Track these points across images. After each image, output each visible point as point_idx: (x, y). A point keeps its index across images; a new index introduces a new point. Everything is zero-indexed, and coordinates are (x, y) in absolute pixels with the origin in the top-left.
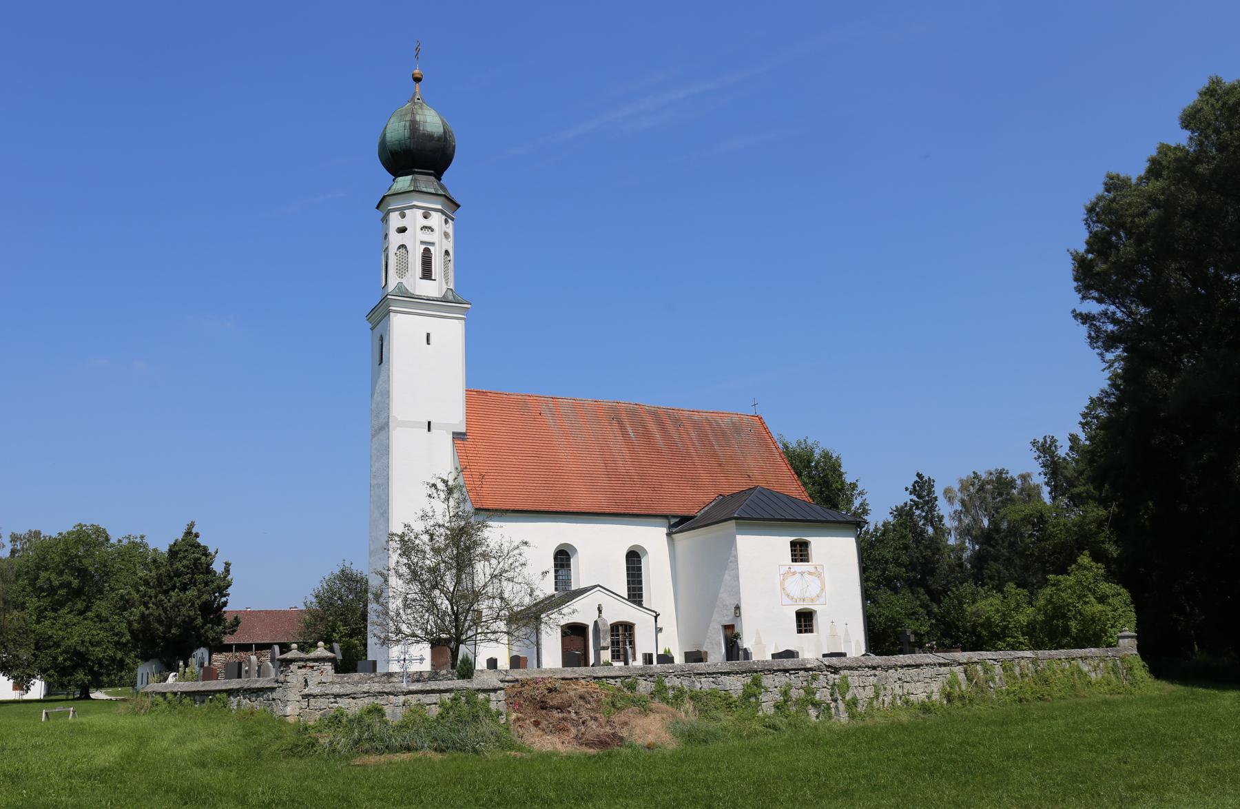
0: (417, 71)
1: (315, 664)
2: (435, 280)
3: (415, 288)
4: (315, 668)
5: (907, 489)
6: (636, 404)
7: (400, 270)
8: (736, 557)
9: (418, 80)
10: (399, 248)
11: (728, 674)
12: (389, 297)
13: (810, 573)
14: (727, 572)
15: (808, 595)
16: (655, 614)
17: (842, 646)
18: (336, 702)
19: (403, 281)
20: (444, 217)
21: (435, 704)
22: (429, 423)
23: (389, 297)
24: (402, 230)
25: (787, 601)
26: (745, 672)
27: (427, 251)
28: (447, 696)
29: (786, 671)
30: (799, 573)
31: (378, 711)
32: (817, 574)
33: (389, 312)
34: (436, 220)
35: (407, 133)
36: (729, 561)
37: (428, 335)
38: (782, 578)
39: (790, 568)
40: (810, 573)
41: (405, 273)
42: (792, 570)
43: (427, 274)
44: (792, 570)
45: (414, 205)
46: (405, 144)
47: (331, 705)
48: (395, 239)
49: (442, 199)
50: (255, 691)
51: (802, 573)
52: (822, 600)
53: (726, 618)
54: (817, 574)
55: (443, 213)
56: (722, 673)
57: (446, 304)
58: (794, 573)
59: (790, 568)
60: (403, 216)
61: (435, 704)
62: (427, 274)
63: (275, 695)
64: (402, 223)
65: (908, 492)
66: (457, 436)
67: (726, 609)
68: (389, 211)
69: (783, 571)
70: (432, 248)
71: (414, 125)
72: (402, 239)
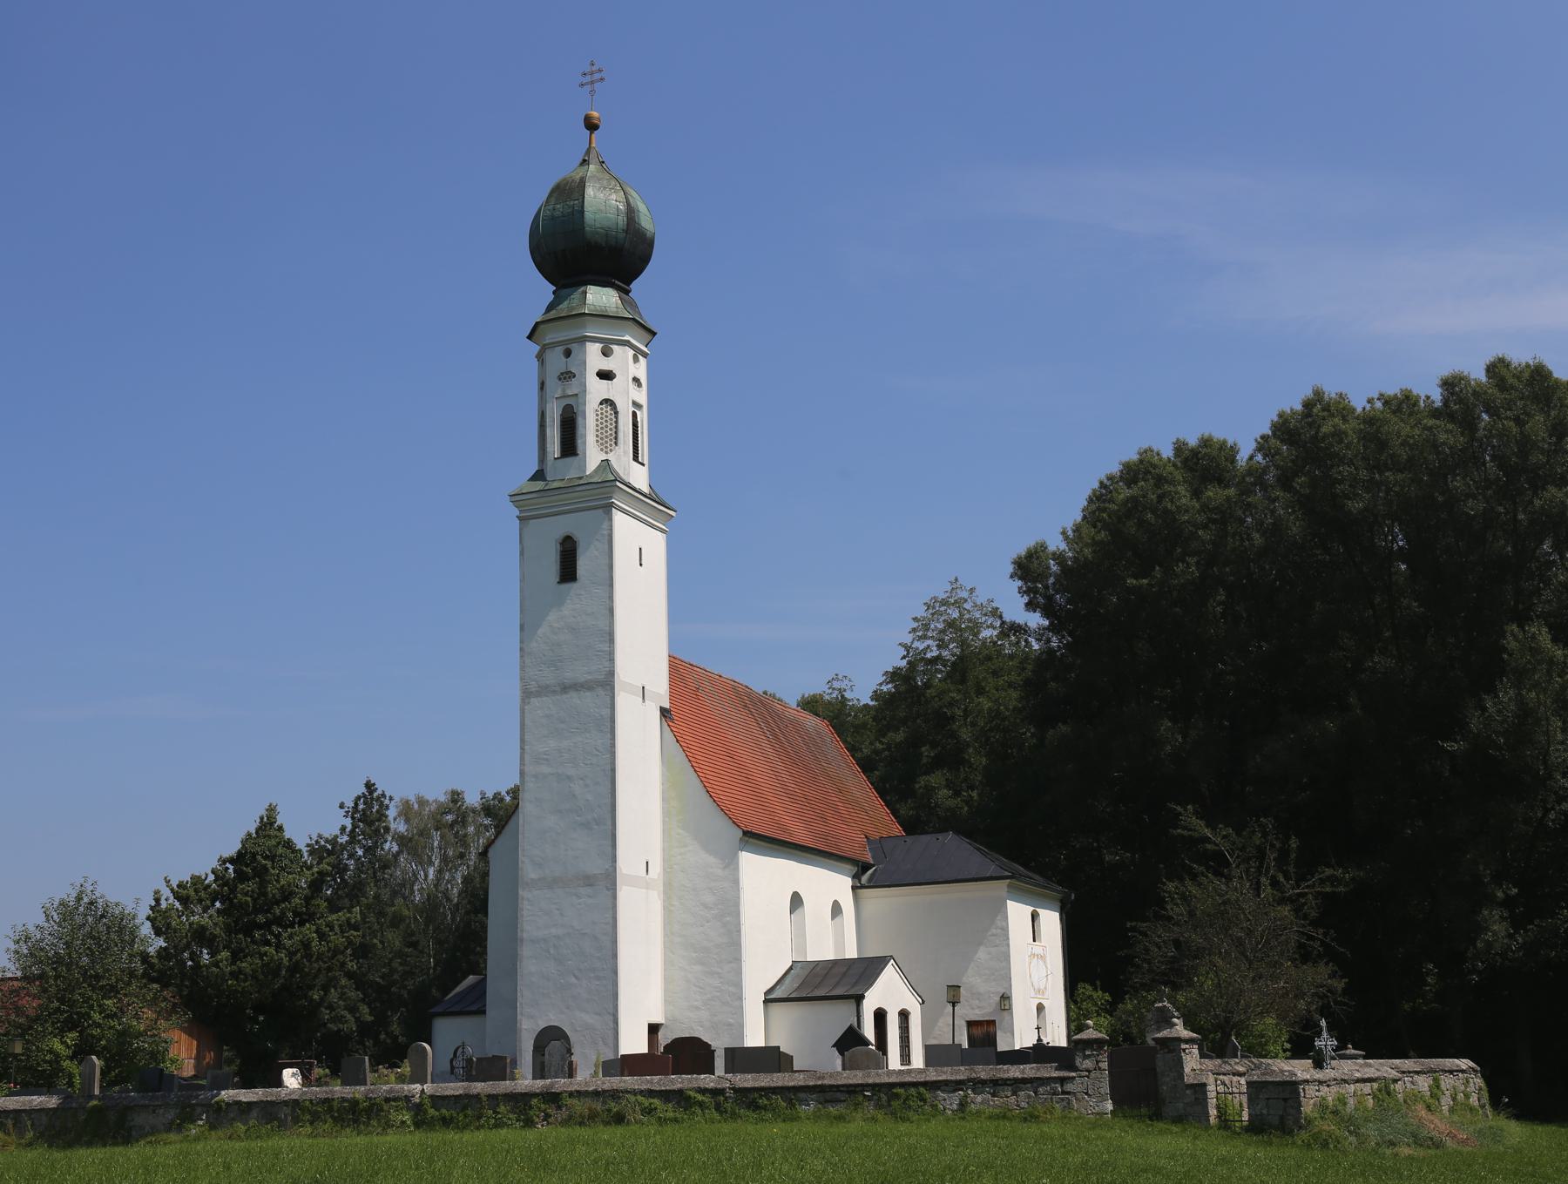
0: (595, 114)
1: (1187, 1046)
2: (643, 465)
3: (629, 474)
4: (1187, 1051)
5: (342, 806)
6: (746, 687)
7: (602, 439)
8: (1005, 930)
9: (591, 126)
10: (601, 403)
11: (1418, 1073)
12: (618, 484)
14: (982, 948)
18: (1318, 1091)
19: (611, 457)
21: (1369, 1094)
22: (643, 688)
23: (618, 484)
24: (606, 375)
26: (1428, 1072)
27: (634, 415)
28: (1375, 1085)
29: (1451, 1072)
31: (1342, 1100)
33: (612, 505)
35: (622, 221)
36: (990, 933)
41: (611, 445)
45: (628, 341)
46: (616, 238)
47: (1317, 1094)
48: (596, 390)
50: (1008, 1082)
53: (977, 1011)
56: (1418, 1073)
57: (655, 504)
60: (606, 353)
61: (1369, 1094)
63: (1069, 1087)
64: (606, 364)
65: (342, 812)
66: (664, 712)
67: (978, 999)
68: (584, 340)
70: (638, 413)
71: (631, 212)
72: (609, 389)
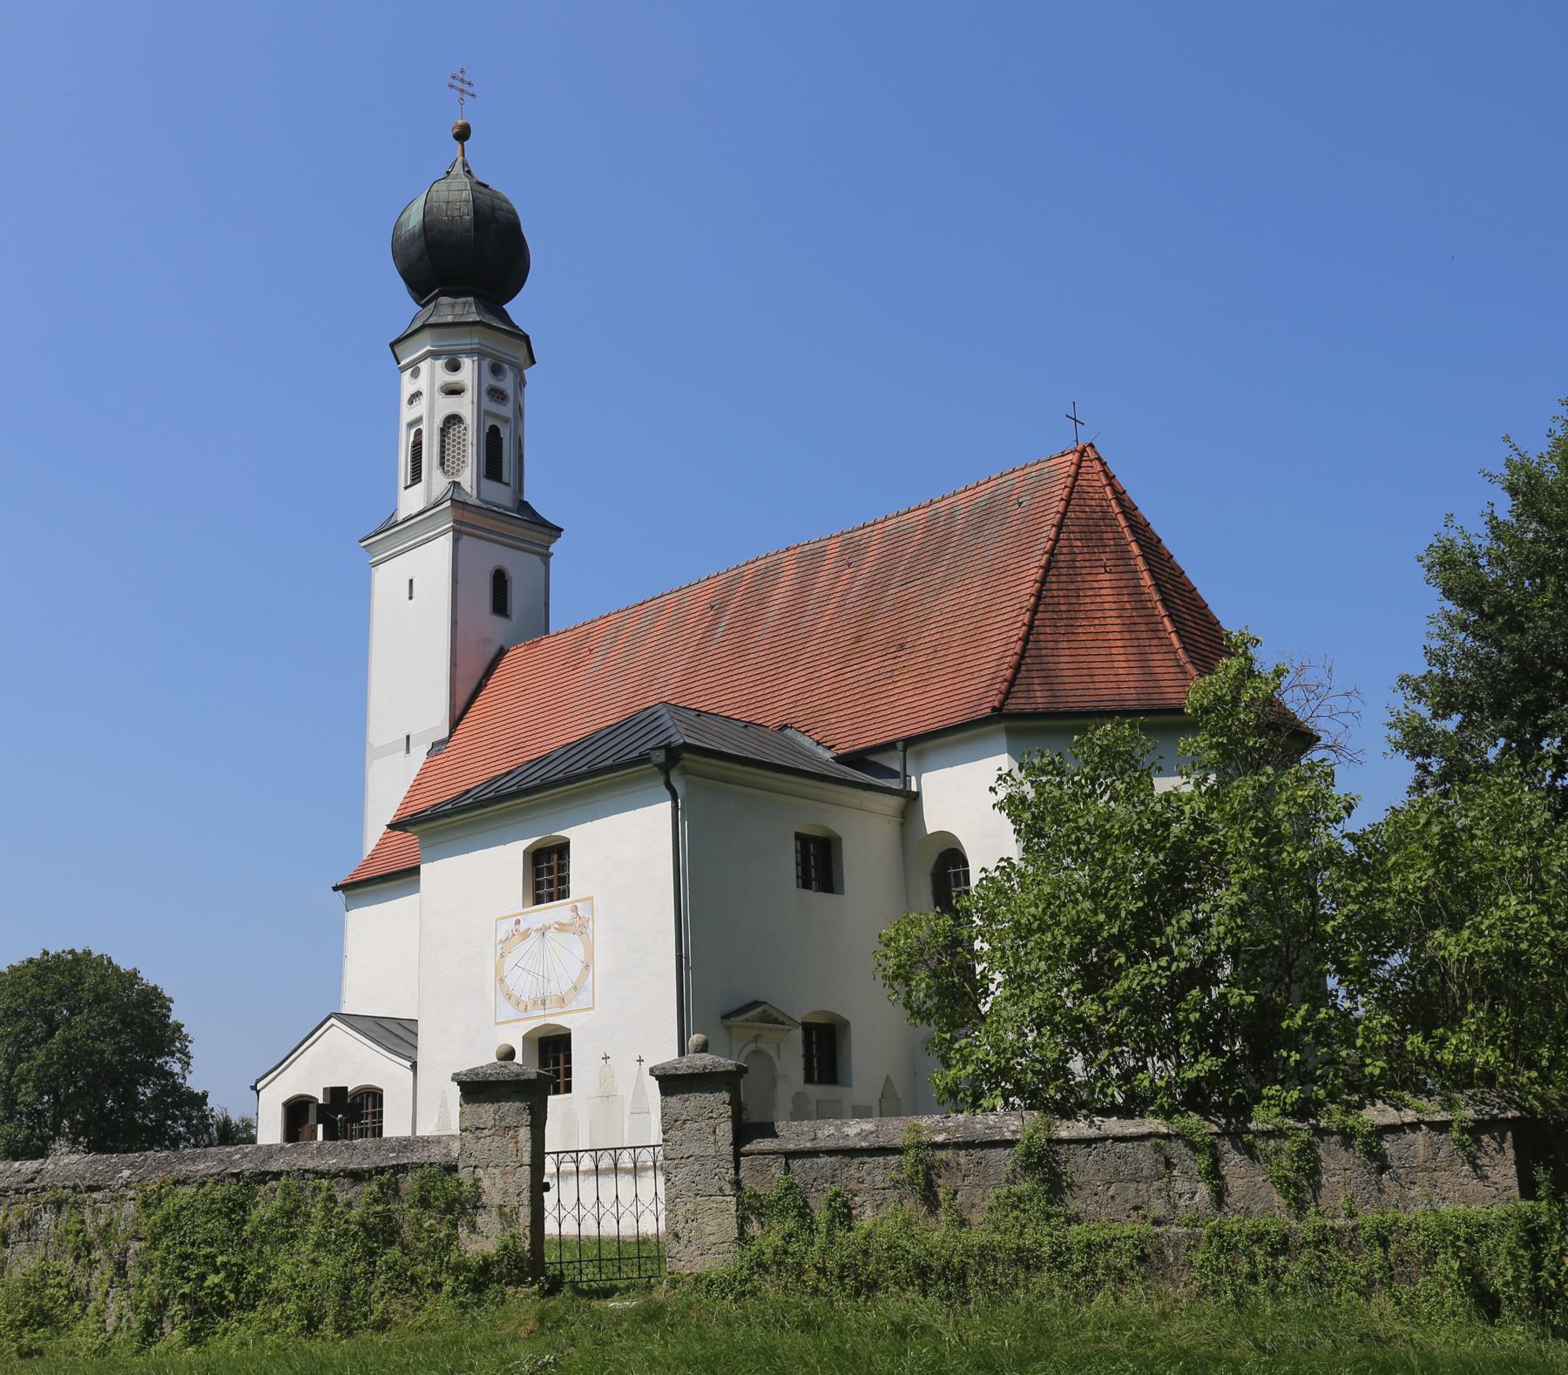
13: (562, 927)
15: (553, 989)
16: (408, 1064)
17: (626, 1122)
20: (440, 363)
25: (508, 1011)
30: (537, 930)
32: (579, 927)
34: (432, 374)
37: (411, 581)
38: (499, 952)
39: (518, 922)
40: (562, 927)
42: (523, 927)
43: (416, 476)
44: (523, 927)
49: (426, 333)
51: (543, 932)
52: (584, 997)
54: (579, 927)
55: (434, 355)
58: (526, 934)
59: (518, 922)
62: (416, 476)
69: (502, 935)
